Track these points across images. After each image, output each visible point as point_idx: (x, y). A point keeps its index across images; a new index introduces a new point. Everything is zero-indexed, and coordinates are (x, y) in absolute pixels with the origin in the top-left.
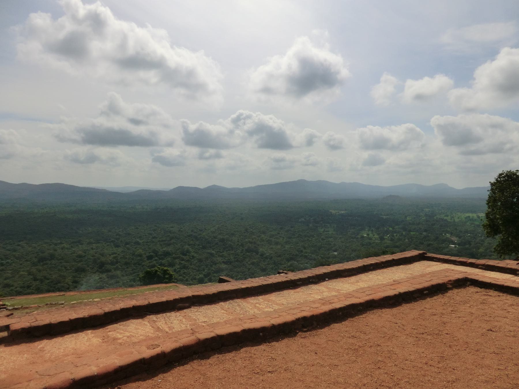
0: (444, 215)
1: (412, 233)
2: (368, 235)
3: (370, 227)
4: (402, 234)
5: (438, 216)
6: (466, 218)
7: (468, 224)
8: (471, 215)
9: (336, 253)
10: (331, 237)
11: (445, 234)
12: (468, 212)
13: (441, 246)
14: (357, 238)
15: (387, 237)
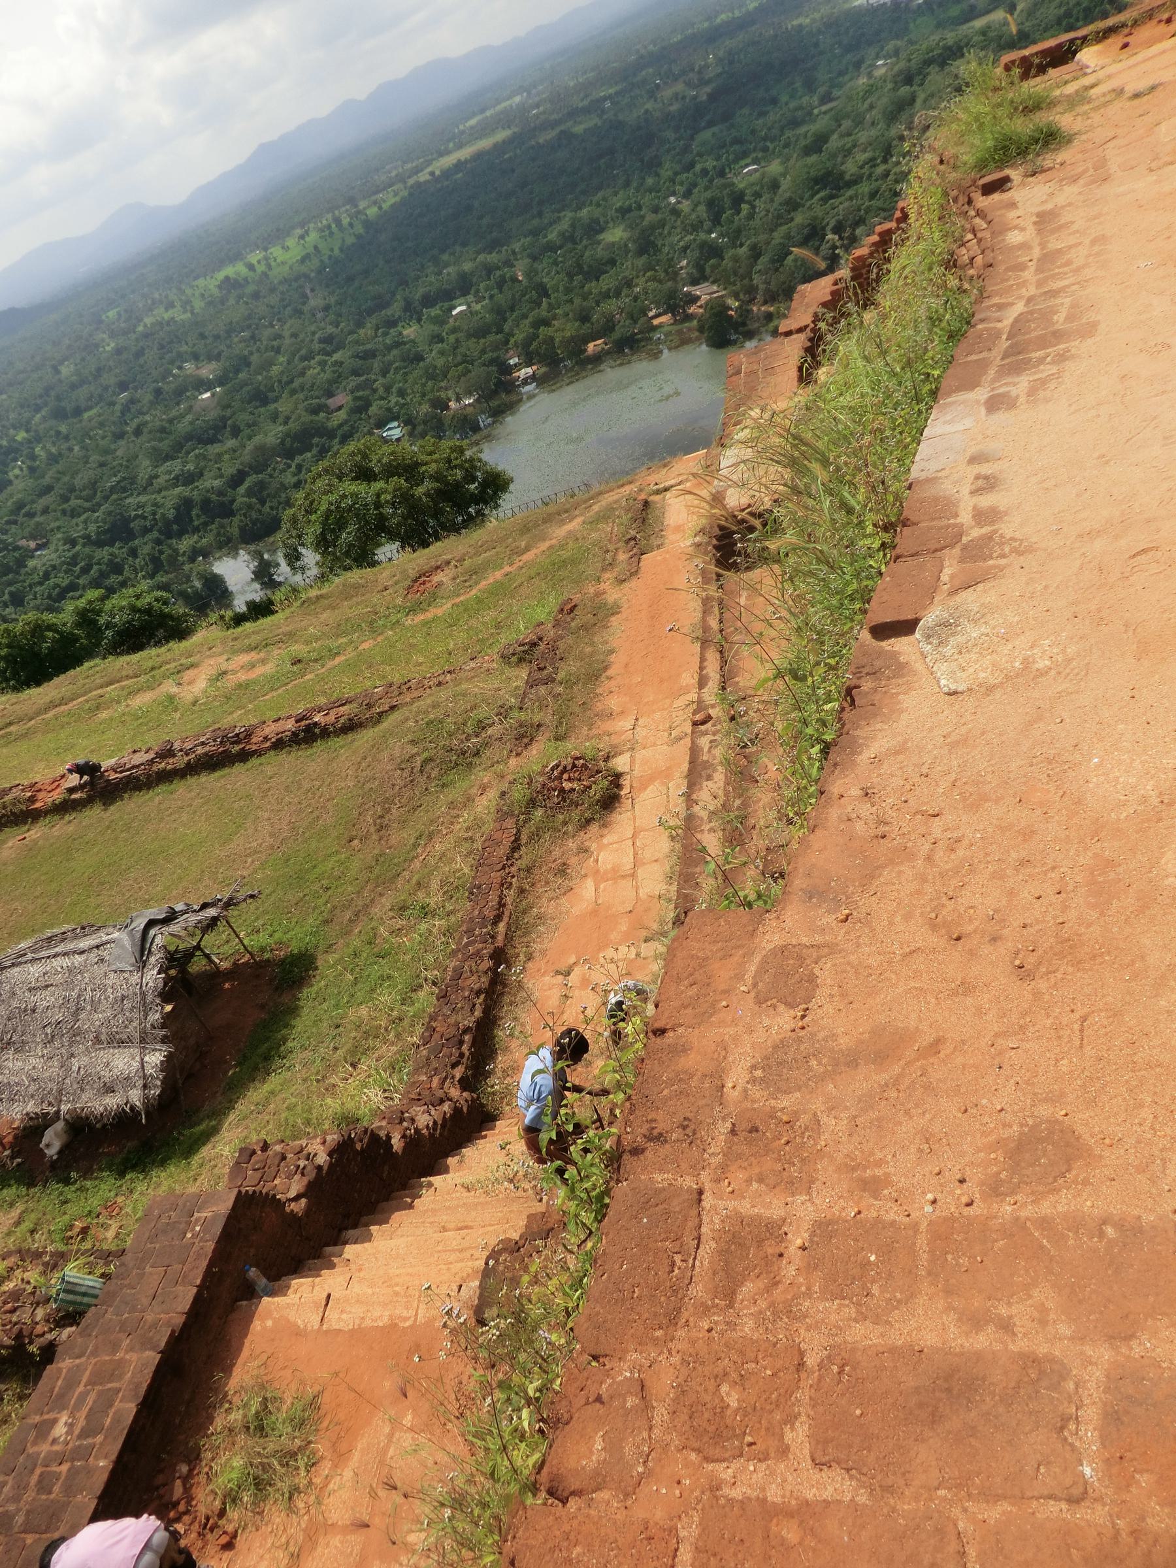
1: (86, 415)
4: (58, 433)
5: (148, 320)
6: (220, 287)
8: (229, 271)
12: (222, 263)
13: (174, 413)
15: (17, 471)
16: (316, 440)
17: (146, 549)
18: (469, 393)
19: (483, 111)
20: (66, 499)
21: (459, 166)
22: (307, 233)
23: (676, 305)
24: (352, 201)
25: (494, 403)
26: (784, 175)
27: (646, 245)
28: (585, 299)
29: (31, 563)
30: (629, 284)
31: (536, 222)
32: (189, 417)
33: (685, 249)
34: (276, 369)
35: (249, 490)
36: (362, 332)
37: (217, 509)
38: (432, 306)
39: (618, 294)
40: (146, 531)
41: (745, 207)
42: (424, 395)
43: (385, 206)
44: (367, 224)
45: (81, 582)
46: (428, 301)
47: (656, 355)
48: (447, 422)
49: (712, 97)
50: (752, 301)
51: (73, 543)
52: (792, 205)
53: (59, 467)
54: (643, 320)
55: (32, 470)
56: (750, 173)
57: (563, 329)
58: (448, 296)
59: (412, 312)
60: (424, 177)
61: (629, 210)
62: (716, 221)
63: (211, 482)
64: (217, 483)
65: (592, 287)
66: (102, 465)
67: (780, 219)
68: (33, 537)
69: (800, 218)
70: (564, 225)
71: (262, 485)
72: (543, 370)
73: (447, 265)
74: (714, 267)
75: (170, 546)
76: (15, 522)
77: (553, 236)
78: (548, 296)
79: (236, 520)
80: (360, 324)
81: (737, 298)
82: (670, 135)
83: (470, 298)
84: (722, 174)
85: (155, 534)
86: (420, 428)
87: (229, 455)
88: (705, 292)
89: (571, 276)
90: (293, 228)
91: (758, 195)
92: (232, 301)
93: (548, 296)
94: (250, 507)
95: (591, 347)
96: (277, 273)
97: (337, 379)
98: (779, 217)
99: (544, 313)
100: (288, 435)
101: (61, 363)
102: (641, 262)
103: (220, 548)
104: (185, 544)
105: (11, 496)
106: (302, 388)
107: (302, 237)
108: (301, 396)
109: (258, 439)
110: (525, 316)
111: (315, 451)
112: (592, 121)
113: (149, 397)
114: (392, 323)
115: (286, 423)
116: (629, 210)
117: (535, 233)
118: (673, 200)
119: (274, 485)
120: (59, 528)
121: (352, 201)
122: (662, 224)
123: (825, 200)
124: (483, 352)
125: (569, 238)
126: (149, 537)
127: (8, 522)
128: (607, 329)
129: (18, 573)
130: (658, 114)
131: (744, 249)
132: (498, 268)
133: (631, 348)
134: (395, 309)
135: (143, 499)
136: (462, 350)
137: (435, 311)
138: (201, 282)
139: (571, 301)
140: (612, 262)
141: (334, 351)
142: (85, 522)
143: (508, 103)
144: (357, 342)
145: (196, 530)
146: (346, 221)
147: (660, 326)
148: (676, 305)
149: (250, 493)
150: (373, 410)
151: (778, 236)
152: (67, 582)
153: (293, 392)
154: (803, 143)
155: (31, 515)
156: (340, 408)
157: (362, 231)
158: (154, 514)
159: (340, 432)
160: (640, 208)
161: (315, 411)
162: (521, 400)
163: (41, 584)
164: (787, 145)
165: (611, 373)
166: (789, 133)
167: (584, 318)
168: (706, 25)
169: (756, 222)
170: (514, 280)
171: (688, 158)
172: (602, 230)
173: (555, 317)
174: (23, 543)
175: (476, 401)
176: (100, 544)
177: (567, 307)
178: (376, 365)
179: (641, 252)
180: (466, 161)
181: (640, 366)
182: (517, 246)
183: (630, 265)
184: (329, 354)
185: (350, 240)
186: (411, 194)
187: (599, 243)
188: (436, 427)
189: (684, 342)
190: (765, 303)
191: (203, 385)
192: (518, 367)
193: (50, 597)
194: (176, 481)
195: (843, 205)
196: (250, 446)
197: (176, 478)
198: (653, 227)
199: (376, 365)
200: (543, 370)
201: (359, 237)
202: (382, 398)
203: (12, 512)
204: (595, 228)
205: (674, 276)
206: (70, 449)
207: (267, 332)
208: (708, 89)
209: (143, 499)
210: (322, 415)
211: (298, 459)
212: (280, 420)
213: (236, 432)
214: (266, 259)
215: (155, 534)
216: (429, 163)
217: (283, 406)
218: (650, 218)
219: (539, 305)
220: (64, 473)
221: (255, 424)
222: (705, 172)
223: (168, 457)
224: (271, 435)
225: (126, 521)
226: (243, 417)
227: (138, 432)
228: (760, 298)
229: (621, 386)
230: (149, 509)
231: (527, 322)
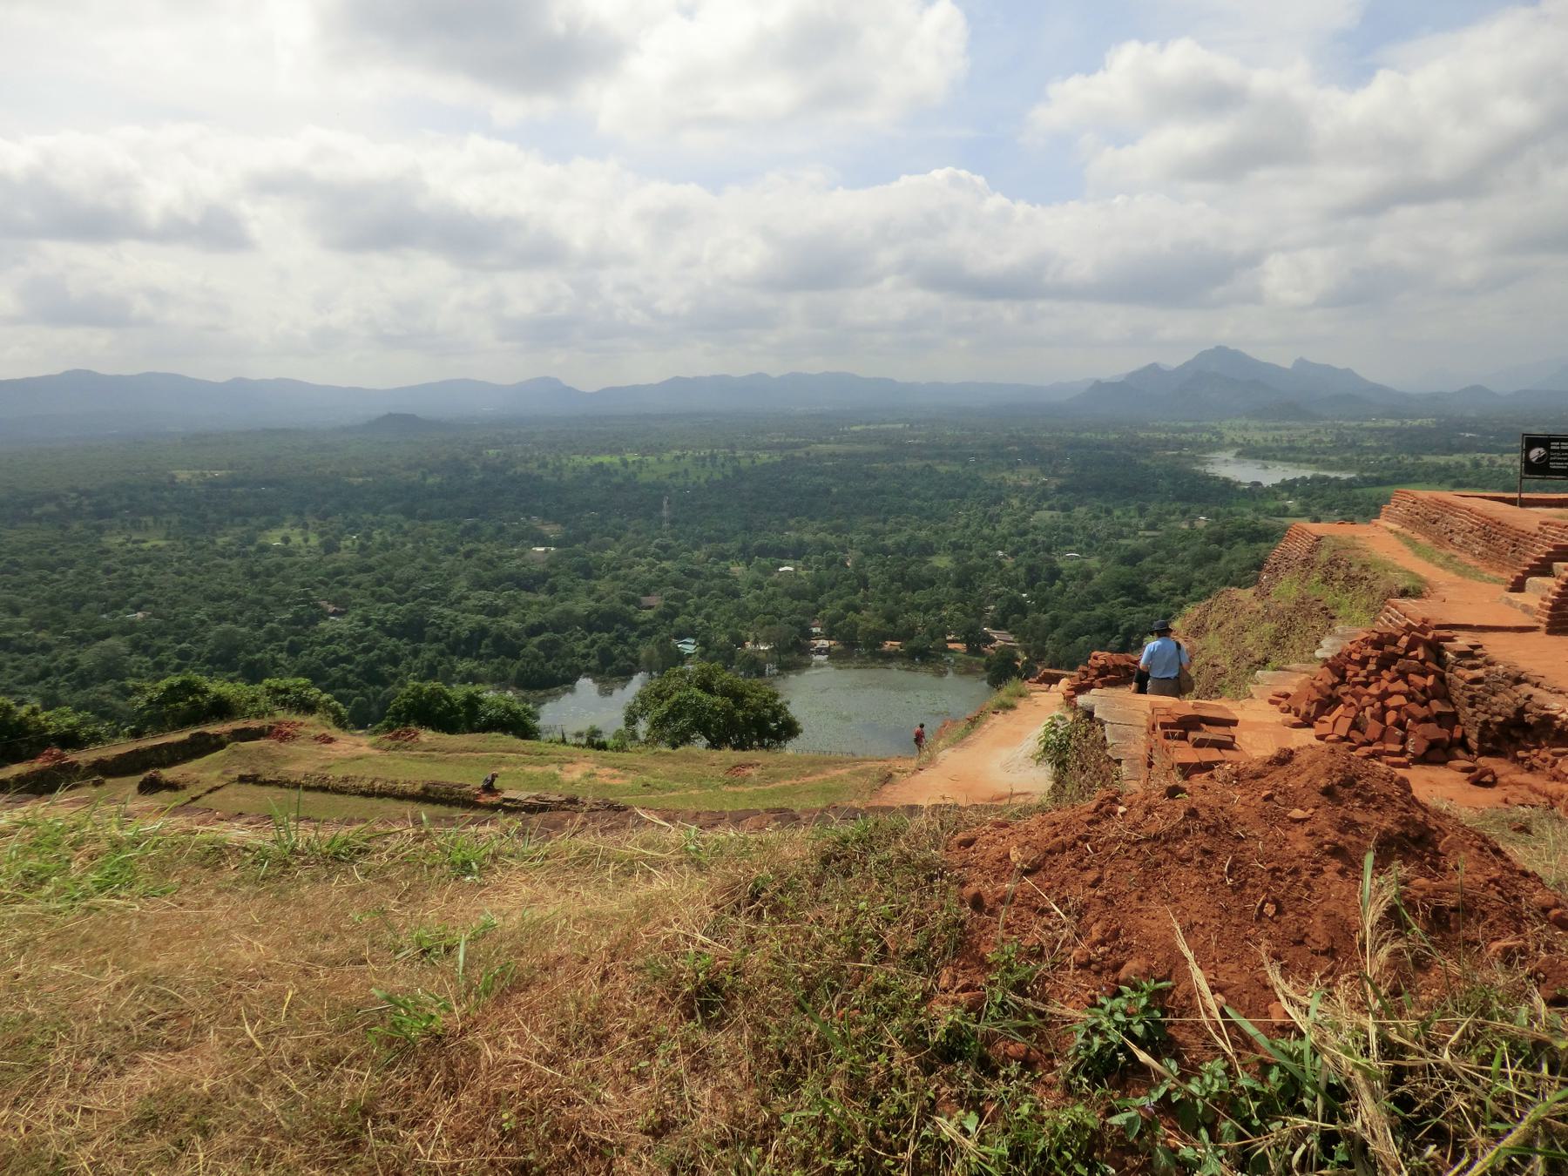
0: (535, 465)
2: (286, 540)
3: (300, 513)
4: (400, 527)
5: (520, 469)
7: (596, 483)
8: (606, 459)
9: (140, 615)
10: (146, 561)
11: (528, 518)
12: (603, 451)
13: (506, 552)
14: (245, 555)
15: (349, 543)
16: (618, 626)
17: (429, 655)
18: (767, 642)
20: (380, 583)
21: (833, 455)
23: (975, 641)
24: (732, 447)
25: (785, 658)
26: (1099, 571)
27: (965, 580)
28: (897, 603)
29: (322, 624)
30: (939, 606)
31: (879, 526)
32: (518, 562)
33: (997, 596)
34: (609, 554)
35: (542, 643)
36: (696, 553)
37: (507, 647)
38: (765, 556)
39: (926, 611)
40: (437, 639)
41: (1059, 583)
42: (727, 627)
43: (758, 462)
44: (737, 471)
45: (358, 658)
46: (763, 551)
47: (941, 674)
48: (739, 657)
50: (1039, 661)
51: (368, 622)
52: (1098, 598)
53: (387, 554)
54: (940, 640)
55: (363, 547)
56: (1072, 558)
57: (869, 620)
58: (782, 554)
59: (746, 554)
60: (798, 453)
61: (961, 547)
62: (1031, 584)
63: (511, 623)
64: (516, 626)
65: (907, 596)
66: (425, 568)
67: (1083, 605)
68: (335, 603)
69: (1099, 611)
70: (902, 538)
71: (555, 644)
72: (840, 647)
73: (790, 529)
74: (1015, 621)
75: (450, 662)
76: (326, 584)
77: (889, 542)
78: (866, 588)
79: (519, 664)
80: (697, 547)
81: (1027, 653)
82: (1015, 502)
83: (800, 563)
84: (1048, 550)
85: (442, 646)
86: (712, 653)
87: (537, 606)
88: (1001, 638)
89: (892, 580)
90: (673, 448)
91: (1073, 578)
92: (596, 483)
93: (866, 588)
94: (536, 658)
95: (889, 645)
96: (645, 477)
97: (658, 584)
98: (1085, 603)
99: (858, 602)
100: (596, 611)
101: (431, 472)
102: (955, 592)
103: (493, 682)
104: (464, 665)
105: (335, 561)
106: (625, 578)
107: (678, 458)
108: (622, 584)
109: (568, 604)
110: (840, 597)
111: (613, 634)
112: (956, 468)
113: (490, 530)
114: (723, 557)
115: (598, 601)
116: (961, 547)
117: (874, 533)
118: (1000, 553)
119: (565, 648)
120: (362, 605)
121: (732, 447)
122: (985, 569)
123: (1125, 605)
124: (793, 611)
125: (902, 549)
126: (435, 646)
127: (321, 582)
128: (907, 635)
129: (306, 627)
131: (1046, 617)
132: (833, 549)
133: (922, 659)
134: (732, 546)
135: (447, 612)
136: (776, 603)
137: (765, 562)
138: (578, 458)
139: (884, 601)
140: (932, 583)
141: (668, 559)
142: (387, 610)
143: (891, 426)
144: (689, 560)
145: (479, 657)
146: (720, 460)
147: (953, 651)
148: (975, 641)
149: (541, 646)
150: (678, 621)
151: (1078, 618)
152: (346, 653)
153: (616, 578)
154: (1122, 552)
155: (343, 584)
156: (650, 607)
157: (730, 474)
158: (450, 628)
159: (642, 628)
160: (970, 549)
161: (628, 601)
162: (808, 665)
163: (322, 645)
164: (1108, 549)
165: (896, 673)
167: (891, 619)
168: (1072, 435)
169: (1064, 599)
170: (843, 564)
172: (934, 553)
173: (866, 608)
174: (324, 603)
175: (771, 650)
176: (390, 633)
177: (879, 605)
178: (697, 585)
179: (958, 585)
181: (924, 677)
182: (856, 538)
183: (945, 591)
184: (660, 560)
185: (718, 476)
186: (783, 463)
187: (926, 563)
188: (728, 657)
189: (969, 671)
190: (1050, 667)
191: (542, 540)
192: (818, 636)
193: (324, 659)
194: (481, 610)
195: (1138, 615)
196: (559, 608)
197: (484, 607)
198: (975, 569)
199: (697, 585)
200: (840, 647)
201: (726, 477)
202: (690, 615)
203: (328, 574)
204: (927, 550)
205: (979, 613)
206: (404, 544)
207: (615, 520)
208: (1058, 481)
209: (447, 612)
210: (632, 608)
211: (595, 635)
212: (594, 596)
213: (552, 590)
214: (641, 462)
215: (442, 646)
217: (603, 586)
218: (975, 561)
219: (856, 593)
220: (388, 561)
221: (571, 590)
222: (1034, 542)
223: (484, 587)
224: (582, 605)
225: (422, 624)
226: (564, 581)
227: (468, 555)
228: (1046, 662)
229: (901, 688)
230: (447, 622)
231: (841, 602)
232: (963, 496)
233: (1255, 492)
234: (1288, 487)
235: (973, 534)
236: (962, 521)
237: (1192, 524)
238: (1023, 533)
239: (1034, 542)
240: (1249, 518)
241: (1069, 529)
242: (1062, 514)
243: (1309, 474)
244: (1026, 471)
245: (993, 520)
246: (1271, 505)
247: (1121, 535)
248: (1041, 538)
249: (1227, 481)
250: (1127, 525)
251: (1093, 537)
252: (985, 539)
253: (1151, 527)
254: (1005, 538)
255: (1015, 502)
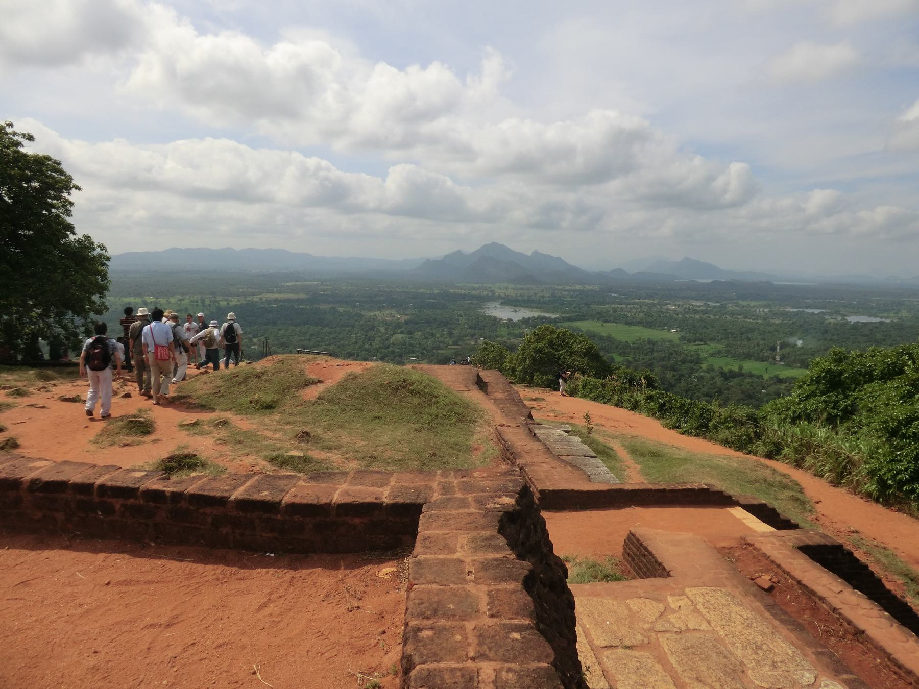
12: (128, 295)
19: (297, 281)
22: (183, 299)
24: (214, 294)
43: (231, 304)
49: (407, 322)
60: (256, 298)
82: (382, 329)
107: (180, 300)
130: (379, 318)
146: (207, 302)
164: (432, 356)
166: (435, 351)
171: (387, 343)
180: (280, 301)
208: (406, 318)
216: (261, 293)
222: (393, 352)
232: (353, 326)
233: (510, 323)
234: (526, 322)
235: (360, 347)
236: (353, 340)
237: (476, 342)
238: (388, 347)
239: (393, 352)
240: (505, 339)
241: (411, 345)
242: (408, 336)
243: (535, 314)
244: (388, 312)
245: (371, 339)
246: (517, 332)
247: (439, 348)
248: (396, 350)
249: (495, 318)
250: (443, 343)
251: (425, 349)
252: (366, 350)
253: (455, 343)
254: (377, 350)
255: (382, 329)
